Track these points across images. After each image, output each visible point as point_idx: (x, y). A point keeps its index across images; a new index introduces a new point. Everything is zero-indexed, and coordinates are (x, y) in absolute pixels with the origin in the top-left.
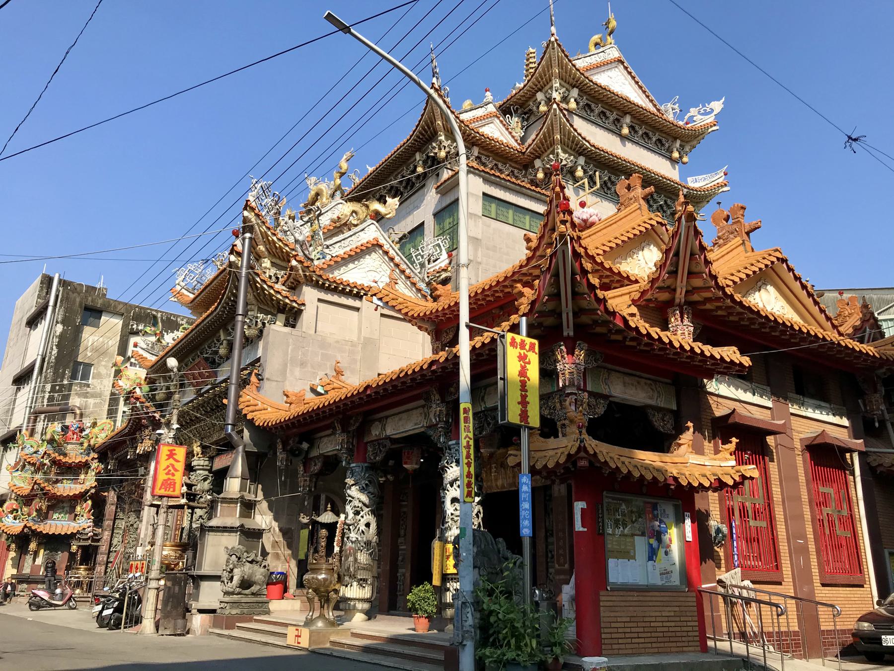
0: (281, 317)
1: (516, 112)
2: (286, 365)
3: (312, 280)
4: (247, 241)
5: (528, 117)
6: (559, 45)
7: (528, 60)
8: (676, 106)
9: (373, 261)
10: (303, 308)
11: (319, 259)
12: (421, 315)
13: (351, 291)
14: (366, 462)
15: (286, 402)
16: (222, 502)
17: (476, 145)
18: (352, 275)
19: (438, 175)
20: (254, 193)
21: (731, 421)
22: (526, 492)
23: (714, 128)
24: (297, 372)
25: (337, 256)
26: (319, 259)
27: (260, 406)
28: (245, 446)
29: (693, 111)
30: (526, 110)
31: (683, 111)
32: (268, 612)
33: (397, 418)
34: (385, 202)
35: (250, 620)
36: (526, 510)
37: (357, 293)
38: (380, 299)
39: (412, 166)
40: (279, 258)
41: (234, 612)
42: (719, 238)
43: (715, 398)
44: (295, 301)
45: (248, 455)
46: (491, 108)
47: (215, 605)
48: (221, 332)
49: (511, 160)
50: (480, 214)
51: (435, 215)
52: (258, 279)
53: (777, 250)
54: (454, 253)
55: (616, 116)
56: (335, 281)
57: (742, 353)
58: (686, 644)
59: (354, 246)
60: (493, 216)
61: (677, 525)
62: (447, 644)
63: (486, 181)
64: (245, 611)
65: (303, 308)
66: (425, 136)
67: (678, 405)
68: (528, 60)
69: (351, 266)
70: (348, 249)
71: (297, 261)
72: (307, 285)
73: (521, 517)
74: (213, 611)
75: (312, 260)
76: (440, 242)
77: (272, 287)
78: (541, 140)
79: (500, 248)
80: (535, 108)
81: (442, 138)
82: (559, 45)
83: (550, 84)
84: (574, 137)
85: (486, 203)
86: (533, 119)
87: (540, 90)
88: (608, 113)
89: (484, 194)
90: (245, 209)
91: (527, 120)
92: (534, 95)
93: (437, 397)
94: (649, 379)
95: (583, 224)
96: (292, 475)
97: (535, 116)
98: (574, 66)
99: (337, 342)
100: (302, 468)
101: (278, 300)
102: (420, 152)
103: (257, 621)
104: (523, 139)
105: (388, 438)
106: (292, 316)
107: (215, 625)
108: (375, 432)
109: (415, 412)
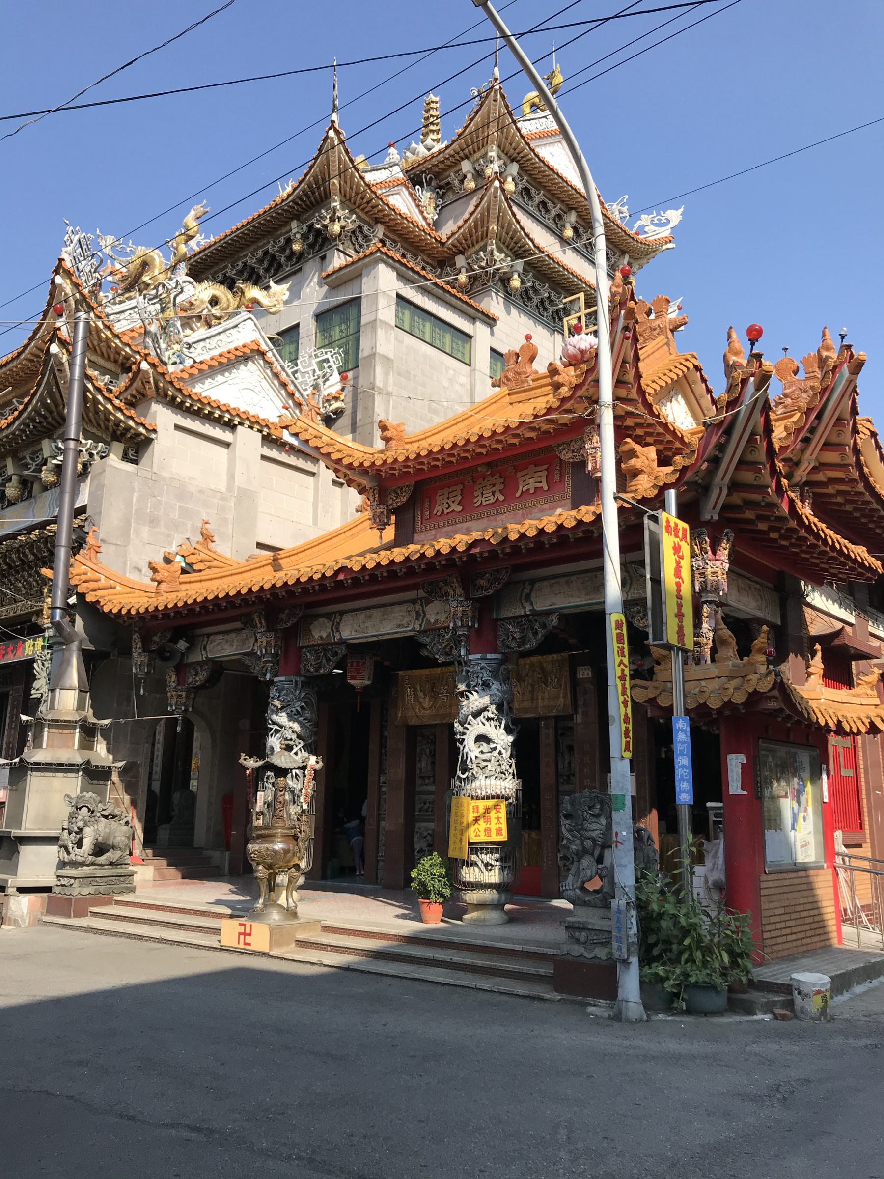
0: (118, 447)
1: (429, 184)
2: (129, 522)
3: (166, 395)
4: (81, 326)
5: (444, 193)
6: (503, 97)
7: (427, 111)
8: (625, 209)
9: (250, 374)
10: (153, 436)
11: (175, 363)
12: (367, 464)
13: (221, 417)
14: (299, 675)
15: (153, 580)
16: (50, 726)
17: (383, 223)
18: (218, 391)
19: (323, 258)
20: (69, 249)
21: (837, 642)
22: (683, 743)
23: (670, 245)
24: (145, 532)
25: (201, 362)
26: (175, 363)
27: (103, 582)
28: (81, 642)
29: (645, 219)
30: (443, 183)
31: (634, 216)
32: (132, 890)
33: (362, 616)
34: (267, 288)
35: (109, 902)
36: (683, 767)
37: (228, 420)
38: (296, 435)
39: (282, 240)
40: (102, 355)
41: (86, 891)
42: (786, 396)
43: (814, 613)
44: (143, 425)
45: (87, 657)
46: (397, 173)
47: (47, 878)
48: (9, 462)
49: (423, 251)
50: (393, 324)
51: (319, 317)
52: (90, 386)
53: (869, 421)
54: (350, 375)
55: (559, 211)
56: (199, 400)
57: (869, 552)
58: (809, 934)
59: (225, 350)
60: (407, 328)
61: (813, 781)
62: (557, 952)
63: (401, 276)
64: (101, 889)
65: (153, 436)
66: (311, 199)
67: (783, 617)
68: (427, 111)
69: (219, 378)
70: (216, 353)
71: (149, 364)
72: (157, 402)
73: (677, 778)
74: (48, 889)
75: (165, 364)
76: (329, 356)
77: (110, 401)
78: (470, 228)
79: (415, 376)
80: (456, 182)
81: (337, 204)
82: (503, 97)
83: (483, 151)
84: (515, 231)
85: (399, 309)
86: (450, 197)
87: (467, 157)
88: (550, 204)
89: (399, 296)
90: (57, 271)
91: (442, 197)
92: (457, 163)
93: (459, 591)
94: (757, 583)
95: (579, 356)
96: (160, 686)
97: (455, 193)
98: (518, 130)
99: (201, 491)
100: (174, 678)
101: (118, 422)
102: (298, 220)
103: (118, 903)
104: (437, 225)
105: (342, 642)
106: (136, 446)
107: (49, 912)
108: (320, 632)
109: (397, 608)
